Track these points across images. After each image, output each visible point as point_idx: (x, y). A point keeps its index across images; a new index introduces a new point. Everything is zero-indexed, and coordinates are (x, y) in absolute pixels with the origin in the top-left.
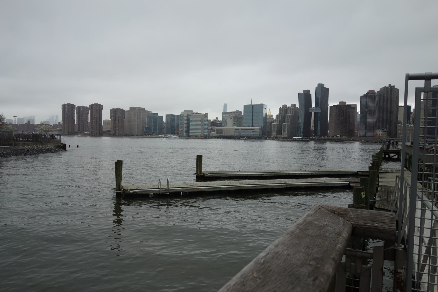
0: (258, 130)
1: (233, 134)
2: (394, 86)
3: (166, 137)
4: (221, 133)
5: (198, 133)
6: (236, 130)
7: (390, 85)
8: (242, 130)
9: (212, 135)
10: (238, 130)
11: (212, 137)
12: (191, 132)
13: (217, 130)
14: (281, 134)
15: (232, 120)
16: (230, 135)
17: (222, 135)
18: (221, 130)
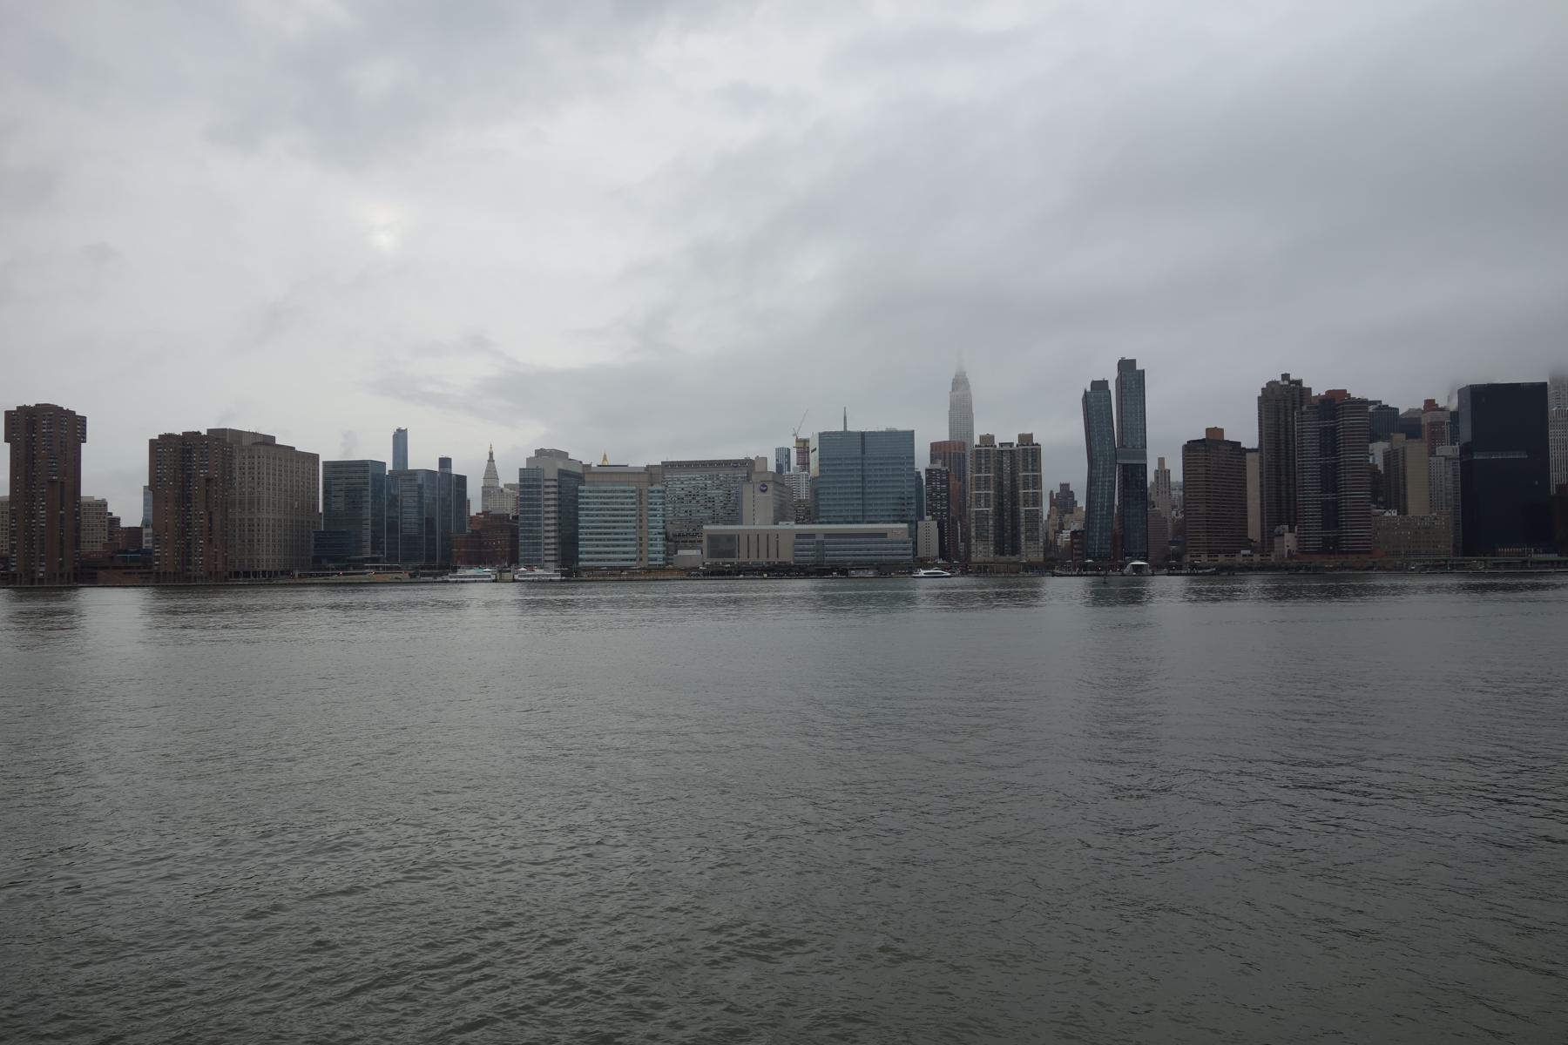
0: (906, 537)
1: (787, 556)
2: (1299, 382)
3: (507, 576)
4: (731, 554)
5: (622, 555)
6: (798, 536)
7: (1285, 376)
8: (829, 535)
9: (680, 565)
10: (812, 536)
11: (690, 573)
12: (587, 553)
13: (714, 539)
14: (1015, 550)
15: (769, 494)
16: (773, 559)
17: (735, 560)
18: (731, 539)
